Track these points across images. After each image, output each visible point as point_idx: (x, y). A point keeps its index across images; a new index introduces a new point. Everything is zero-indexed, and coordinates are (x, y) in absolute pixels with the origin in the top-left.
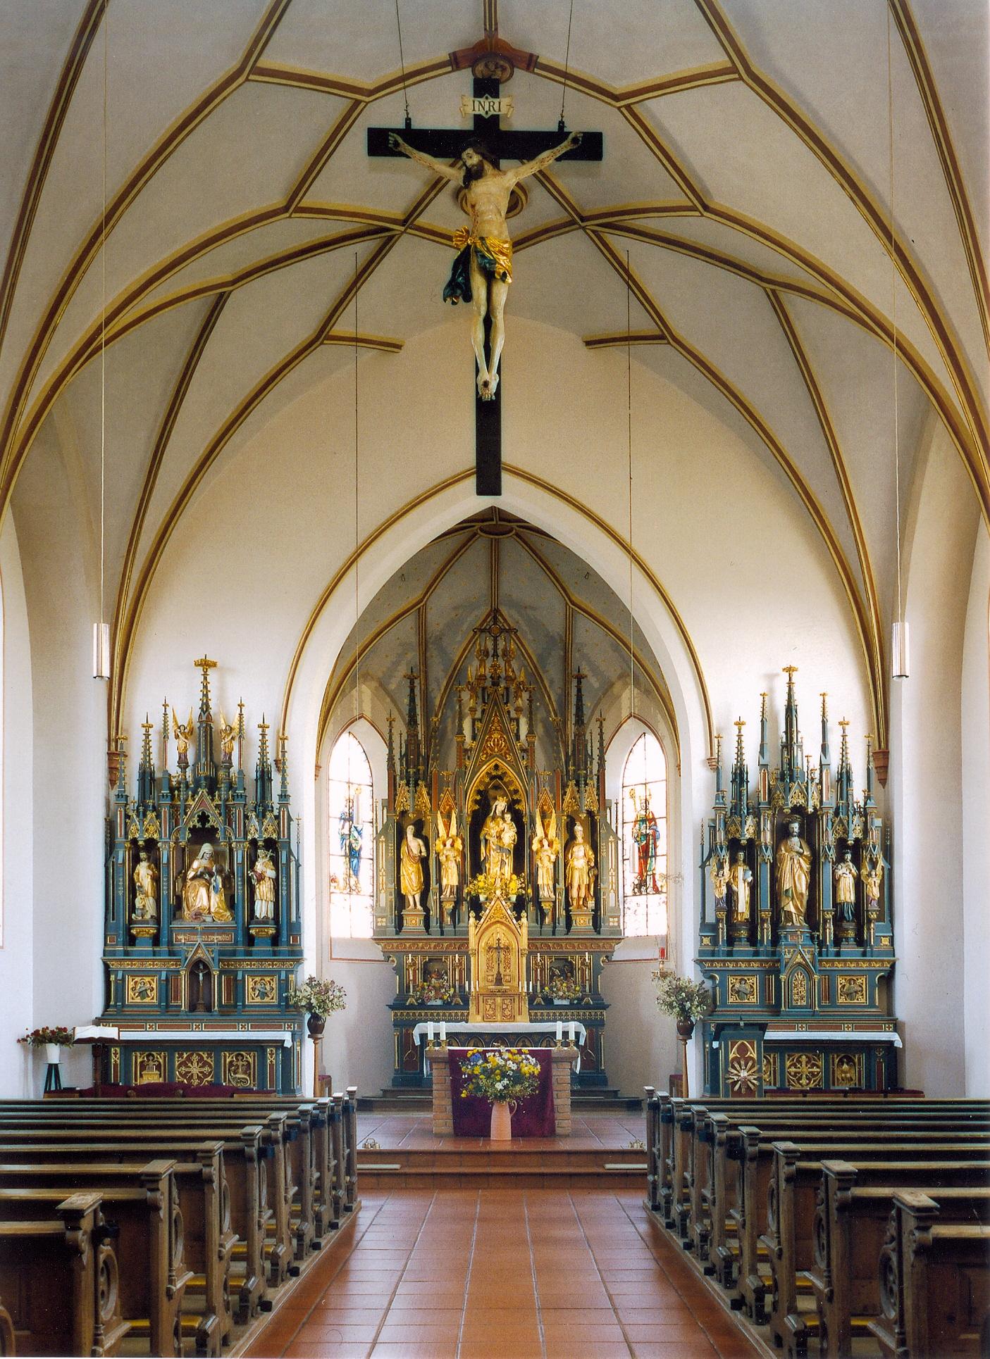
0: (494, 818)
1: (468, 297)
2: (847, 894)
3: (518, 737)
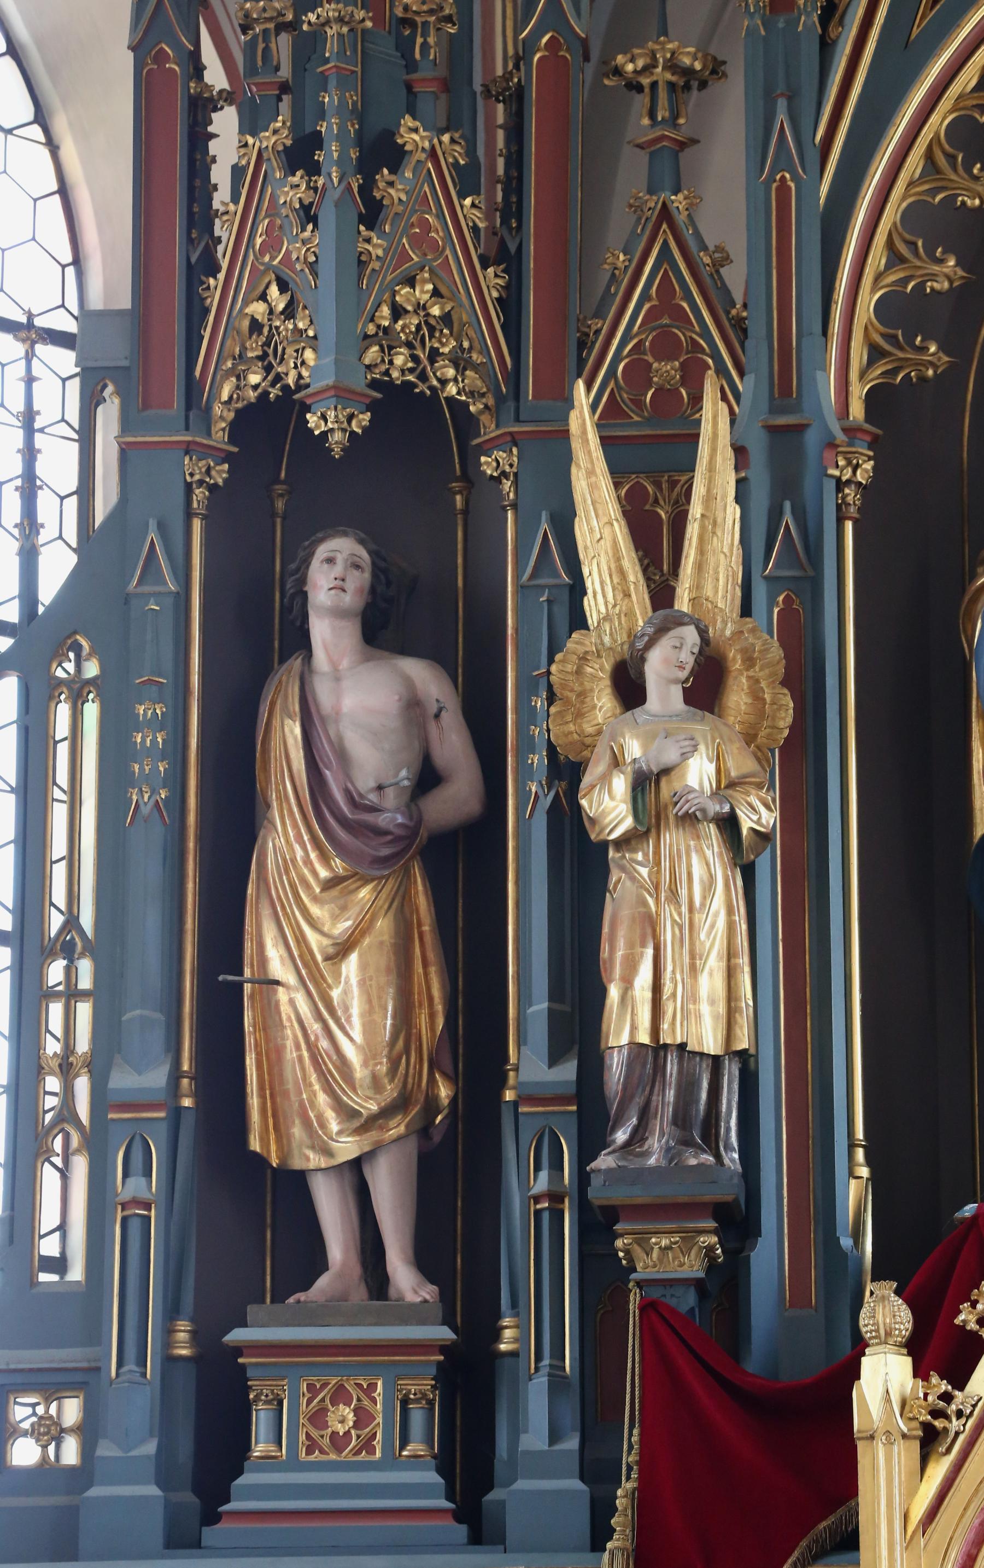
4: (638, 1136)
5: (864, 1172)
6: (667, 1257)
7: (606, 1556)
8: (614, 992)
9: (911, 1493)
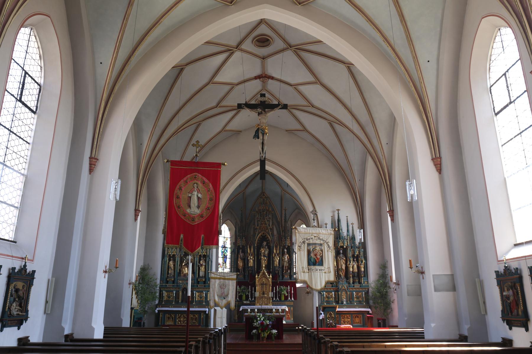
0: (263, 248)
1: (258, 138)
2: (356, 270)
3: (269, 225)
6: (250, 272)
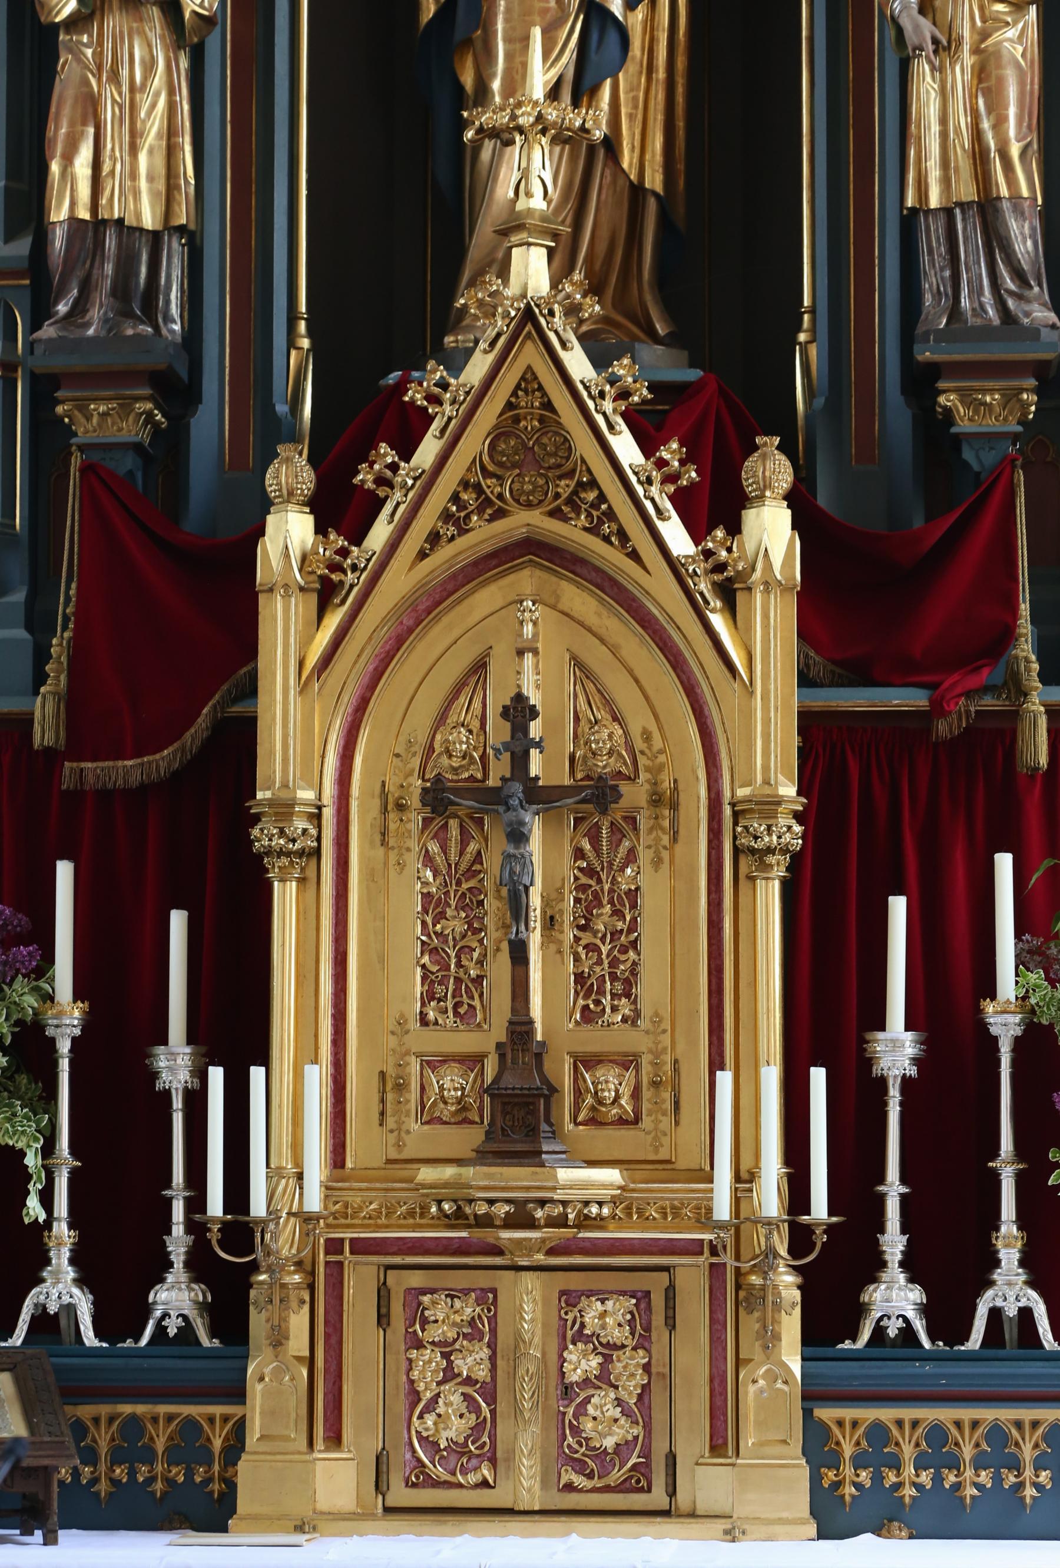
4: (80, 308)
5: (305, 343)
6: (110, 423)
7: (39, 699)
8: (55, 167)
9: (306, 641)
